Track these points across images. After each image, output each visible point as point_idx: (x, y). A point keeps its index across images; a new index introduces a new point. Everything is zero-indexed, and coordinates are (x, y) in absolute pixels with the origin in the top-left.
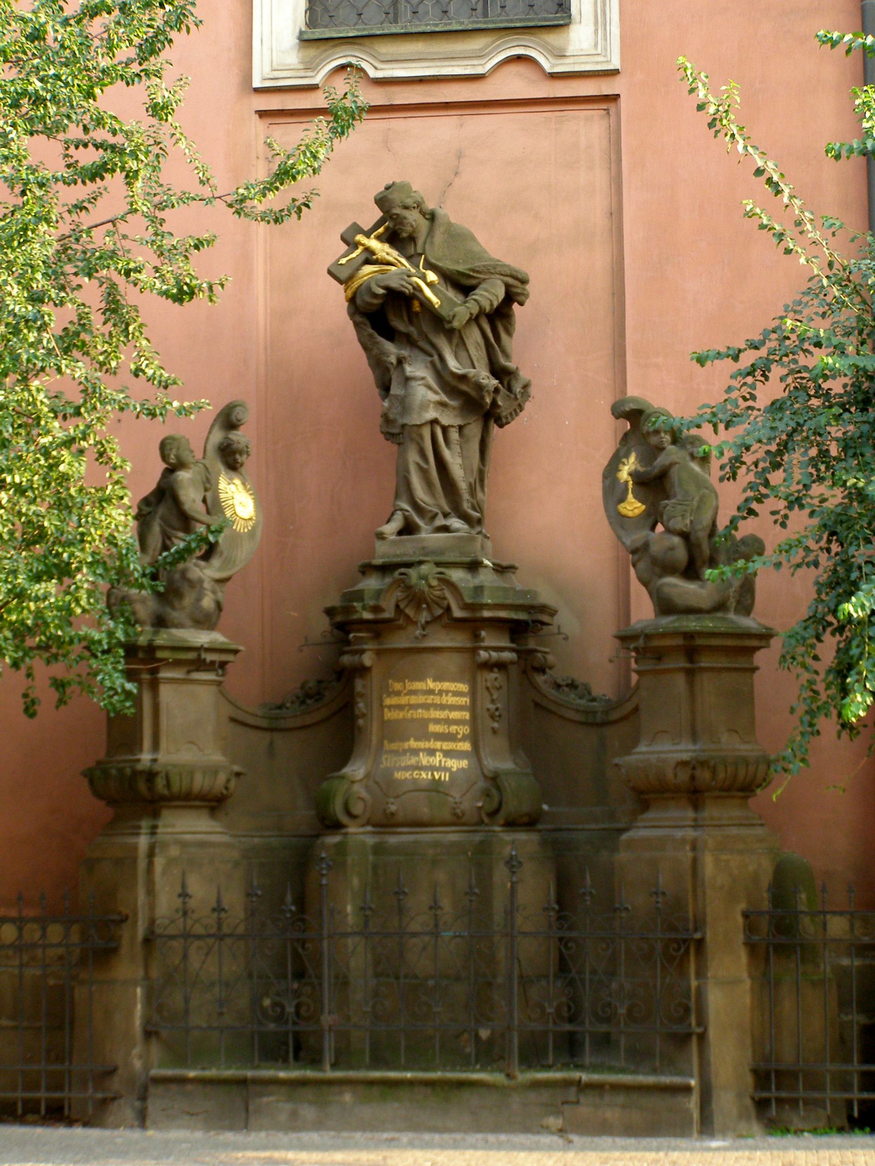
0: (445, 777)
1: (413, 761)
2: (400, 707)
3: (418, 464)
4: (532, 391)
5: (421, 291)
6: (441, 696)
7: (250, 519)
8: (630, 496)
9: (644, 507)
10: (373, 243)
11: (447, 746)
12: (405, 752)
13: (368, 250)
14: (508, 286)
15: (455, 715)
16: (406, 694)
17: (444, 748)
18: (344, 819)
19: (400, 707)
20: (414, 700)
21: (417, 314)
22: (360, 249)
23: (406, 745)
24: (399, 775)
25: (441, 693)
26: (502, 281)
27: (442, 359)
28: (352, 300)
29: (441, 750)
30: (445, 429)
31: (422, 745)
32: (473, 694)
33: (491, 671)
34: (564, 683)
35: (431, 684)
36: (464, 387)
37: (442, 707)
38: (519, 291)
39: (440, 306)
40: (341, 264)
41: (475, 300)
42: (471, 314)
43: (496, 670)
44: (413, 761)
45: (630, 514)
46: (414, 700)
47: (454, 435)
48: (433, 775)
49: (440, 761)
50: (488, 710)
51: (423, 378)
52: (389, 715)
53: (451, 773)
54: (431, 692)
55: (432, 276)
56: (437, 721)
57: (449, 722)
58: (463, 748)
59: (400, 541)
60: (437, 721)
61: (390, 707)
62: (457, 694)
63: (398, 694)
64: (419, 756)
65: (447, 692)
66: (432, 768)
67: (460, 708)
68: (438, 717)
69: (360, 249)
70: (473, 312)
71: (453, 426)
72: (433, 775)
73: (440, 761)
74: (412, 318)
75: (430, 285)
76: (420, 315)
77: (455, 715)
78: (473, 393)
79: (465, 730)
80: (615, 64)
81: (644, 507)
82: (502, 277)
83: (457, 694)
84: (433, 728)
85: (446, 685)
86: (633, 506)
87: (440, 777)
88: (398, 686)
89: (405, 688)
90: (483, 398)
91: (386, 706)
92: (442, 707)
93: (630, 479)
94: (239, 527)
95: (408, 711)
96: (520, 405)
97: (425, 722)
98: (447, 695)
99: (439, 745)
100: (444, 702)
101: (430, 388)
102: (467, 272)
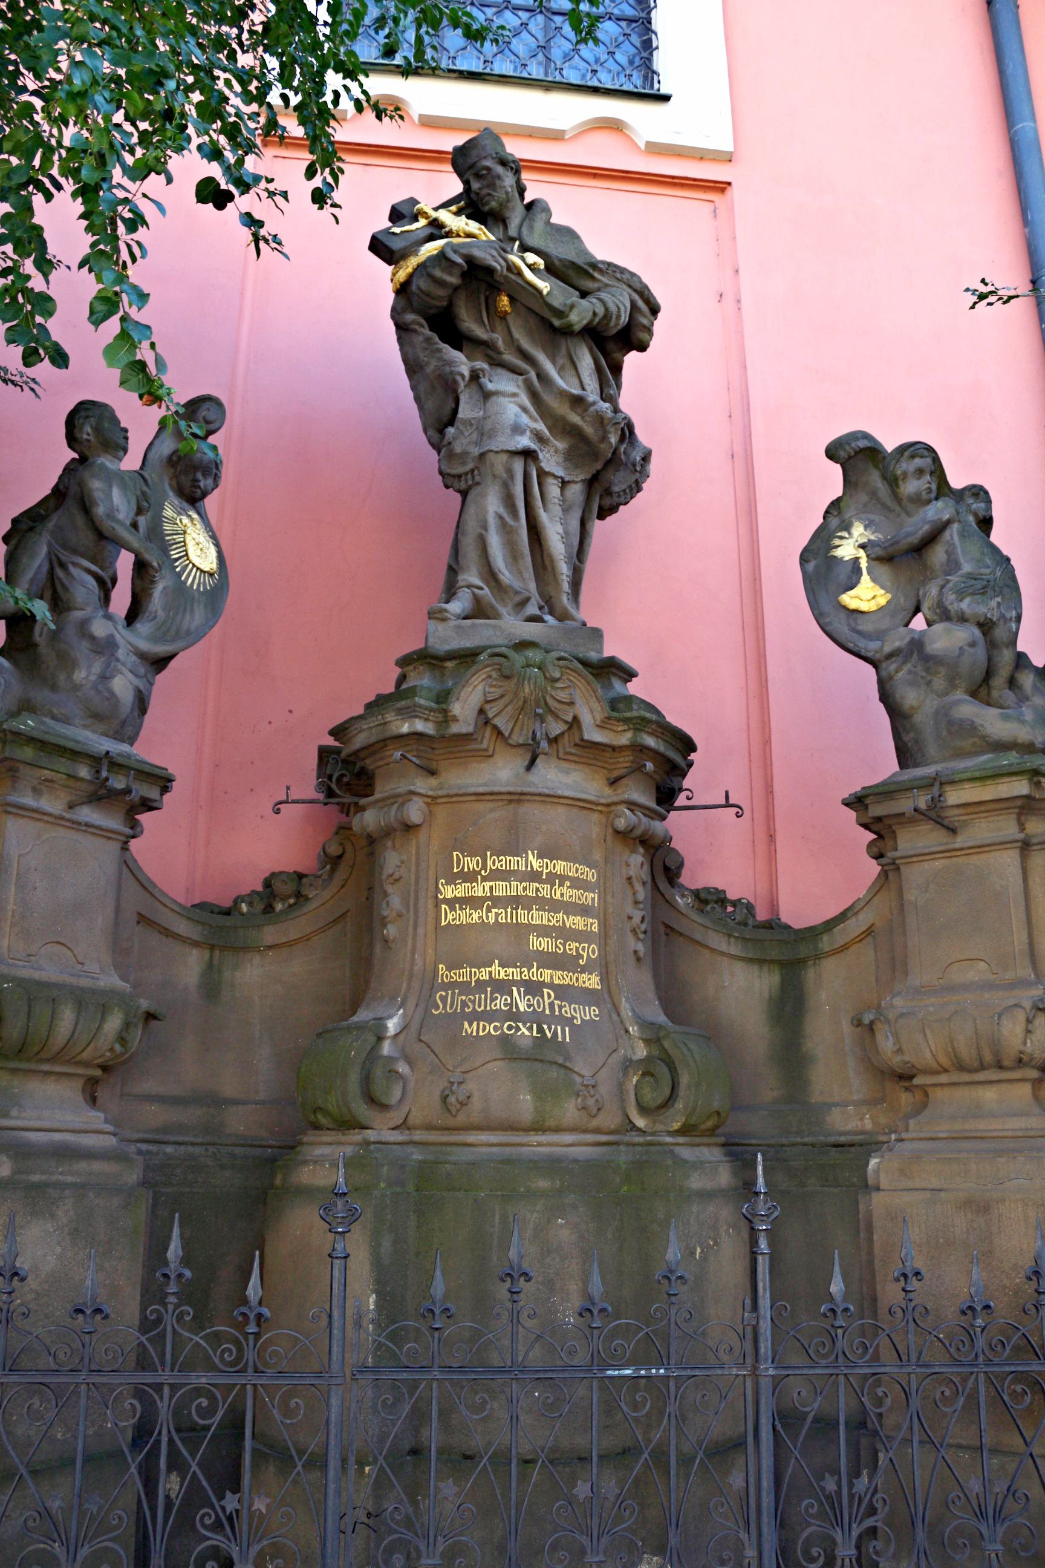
0: (565, 1035)
1: (500, 1003)
2: (473, 902)
3: (501, 518)
4: (654, 466)
5: (520, 273)
6: (553, 885)
7: (211, 575)
8: (865, 578)
9: (889, 596)
10: (445, 216)
11: (560, 977)
12: (481, 985)
13: (435, 224)
14: (634, 305)
15: (577, 922)
16: (484, 879)
17: (556, 981)
18: (362, 1110)
19: (473, 902)
20: (501, 889)
21: (503, 317)
22: (422, 222)
23: (483, 974)
24: (470, 1029)
25: (552, 879)
26: (630, 295)
27: (542, 376)
28: (402, 290)
29: (551, 986)
30: (542, 474)
31: (513, 973)
32: (603, 887)
33: (633, 851)
34: (714, 898)
35: (536, 864)
36: (575, 418)
37: (553, 906)
38: (645, 321)
39: (548, 293)
40: (393, 233)
41: (600, 300)
42: (595, 314)
43: (641, 850)
44: (500, 1003)
45: (864, 607)
46: (501, 889)
47: (553, 489)
48: (540, 1030)
49: (551, 1005)
50: (630, 918)
51: (514, 395)
52: (449, 917)
53: (574, 1029)
54: (534, 876)
55: (531, 258)
56: (544, 931)
57: (564, 933)
58: (587, 984)
59: (473, 626)
60: (544, 931)
61: (452, 903)
62: (577, 883)
63: (470, 877)
64: (511, 994)
65: (563, 878)
66: (537, 1018)
67: (584, 910)
68: (545, 922)
69: (422, 222)
70: (597, 311)
71: (556, 477)
72: (540, 1030)
73: (551, 1005)
74: (496, 317)
75: (532, 267)
76: (509, 317)
77: (577, 922)
78: (589, 430)
79: (590, 951)
80: (728, 146)
81: (889, 596)
82: (629, 290)
83: (577, 883)
84: (537, 943)
85: (560, 866)
86: (867, 595)
87: (555, 1033)
88: (471, 863)
89: (484, 867)
90: (604, 438)
91: (446, 901)
92: (553, 906)
93: (862, 553)
94: (191, 579)
95: (489, 910)
96: (637, 482)
97: (521, 931)
98: (561, 885)
99: (546, 975)
100: (558, 897)
101: (524, 409)
102: (585, 267)
